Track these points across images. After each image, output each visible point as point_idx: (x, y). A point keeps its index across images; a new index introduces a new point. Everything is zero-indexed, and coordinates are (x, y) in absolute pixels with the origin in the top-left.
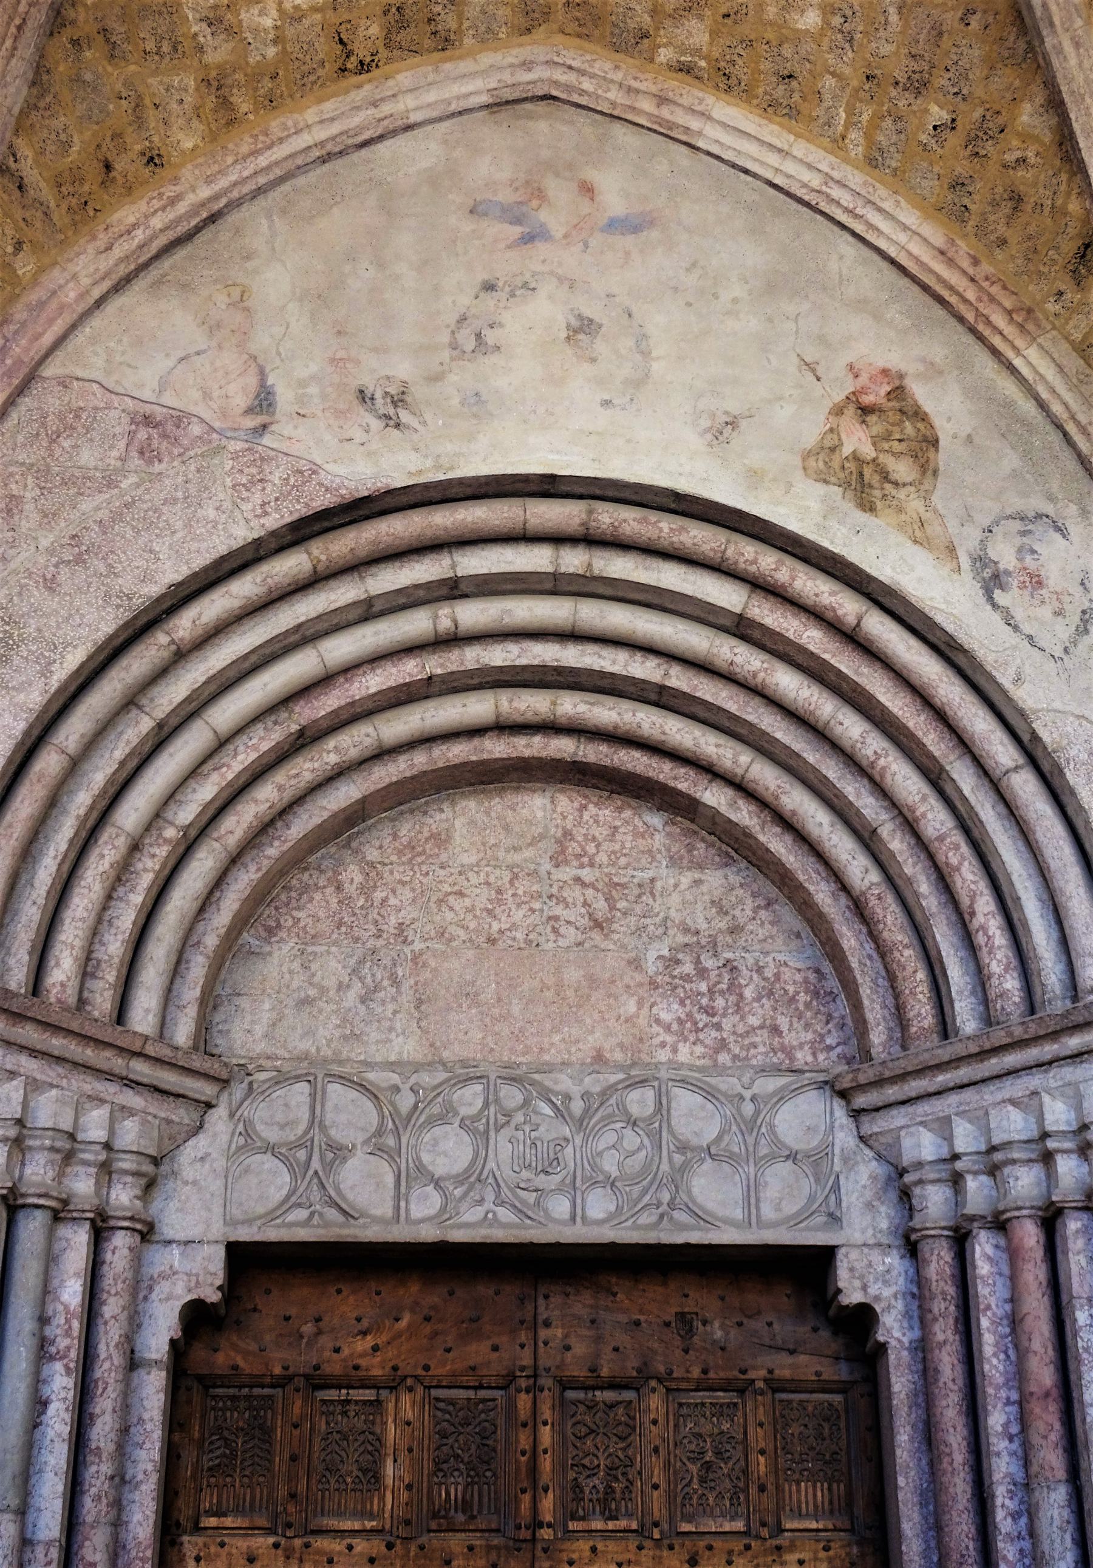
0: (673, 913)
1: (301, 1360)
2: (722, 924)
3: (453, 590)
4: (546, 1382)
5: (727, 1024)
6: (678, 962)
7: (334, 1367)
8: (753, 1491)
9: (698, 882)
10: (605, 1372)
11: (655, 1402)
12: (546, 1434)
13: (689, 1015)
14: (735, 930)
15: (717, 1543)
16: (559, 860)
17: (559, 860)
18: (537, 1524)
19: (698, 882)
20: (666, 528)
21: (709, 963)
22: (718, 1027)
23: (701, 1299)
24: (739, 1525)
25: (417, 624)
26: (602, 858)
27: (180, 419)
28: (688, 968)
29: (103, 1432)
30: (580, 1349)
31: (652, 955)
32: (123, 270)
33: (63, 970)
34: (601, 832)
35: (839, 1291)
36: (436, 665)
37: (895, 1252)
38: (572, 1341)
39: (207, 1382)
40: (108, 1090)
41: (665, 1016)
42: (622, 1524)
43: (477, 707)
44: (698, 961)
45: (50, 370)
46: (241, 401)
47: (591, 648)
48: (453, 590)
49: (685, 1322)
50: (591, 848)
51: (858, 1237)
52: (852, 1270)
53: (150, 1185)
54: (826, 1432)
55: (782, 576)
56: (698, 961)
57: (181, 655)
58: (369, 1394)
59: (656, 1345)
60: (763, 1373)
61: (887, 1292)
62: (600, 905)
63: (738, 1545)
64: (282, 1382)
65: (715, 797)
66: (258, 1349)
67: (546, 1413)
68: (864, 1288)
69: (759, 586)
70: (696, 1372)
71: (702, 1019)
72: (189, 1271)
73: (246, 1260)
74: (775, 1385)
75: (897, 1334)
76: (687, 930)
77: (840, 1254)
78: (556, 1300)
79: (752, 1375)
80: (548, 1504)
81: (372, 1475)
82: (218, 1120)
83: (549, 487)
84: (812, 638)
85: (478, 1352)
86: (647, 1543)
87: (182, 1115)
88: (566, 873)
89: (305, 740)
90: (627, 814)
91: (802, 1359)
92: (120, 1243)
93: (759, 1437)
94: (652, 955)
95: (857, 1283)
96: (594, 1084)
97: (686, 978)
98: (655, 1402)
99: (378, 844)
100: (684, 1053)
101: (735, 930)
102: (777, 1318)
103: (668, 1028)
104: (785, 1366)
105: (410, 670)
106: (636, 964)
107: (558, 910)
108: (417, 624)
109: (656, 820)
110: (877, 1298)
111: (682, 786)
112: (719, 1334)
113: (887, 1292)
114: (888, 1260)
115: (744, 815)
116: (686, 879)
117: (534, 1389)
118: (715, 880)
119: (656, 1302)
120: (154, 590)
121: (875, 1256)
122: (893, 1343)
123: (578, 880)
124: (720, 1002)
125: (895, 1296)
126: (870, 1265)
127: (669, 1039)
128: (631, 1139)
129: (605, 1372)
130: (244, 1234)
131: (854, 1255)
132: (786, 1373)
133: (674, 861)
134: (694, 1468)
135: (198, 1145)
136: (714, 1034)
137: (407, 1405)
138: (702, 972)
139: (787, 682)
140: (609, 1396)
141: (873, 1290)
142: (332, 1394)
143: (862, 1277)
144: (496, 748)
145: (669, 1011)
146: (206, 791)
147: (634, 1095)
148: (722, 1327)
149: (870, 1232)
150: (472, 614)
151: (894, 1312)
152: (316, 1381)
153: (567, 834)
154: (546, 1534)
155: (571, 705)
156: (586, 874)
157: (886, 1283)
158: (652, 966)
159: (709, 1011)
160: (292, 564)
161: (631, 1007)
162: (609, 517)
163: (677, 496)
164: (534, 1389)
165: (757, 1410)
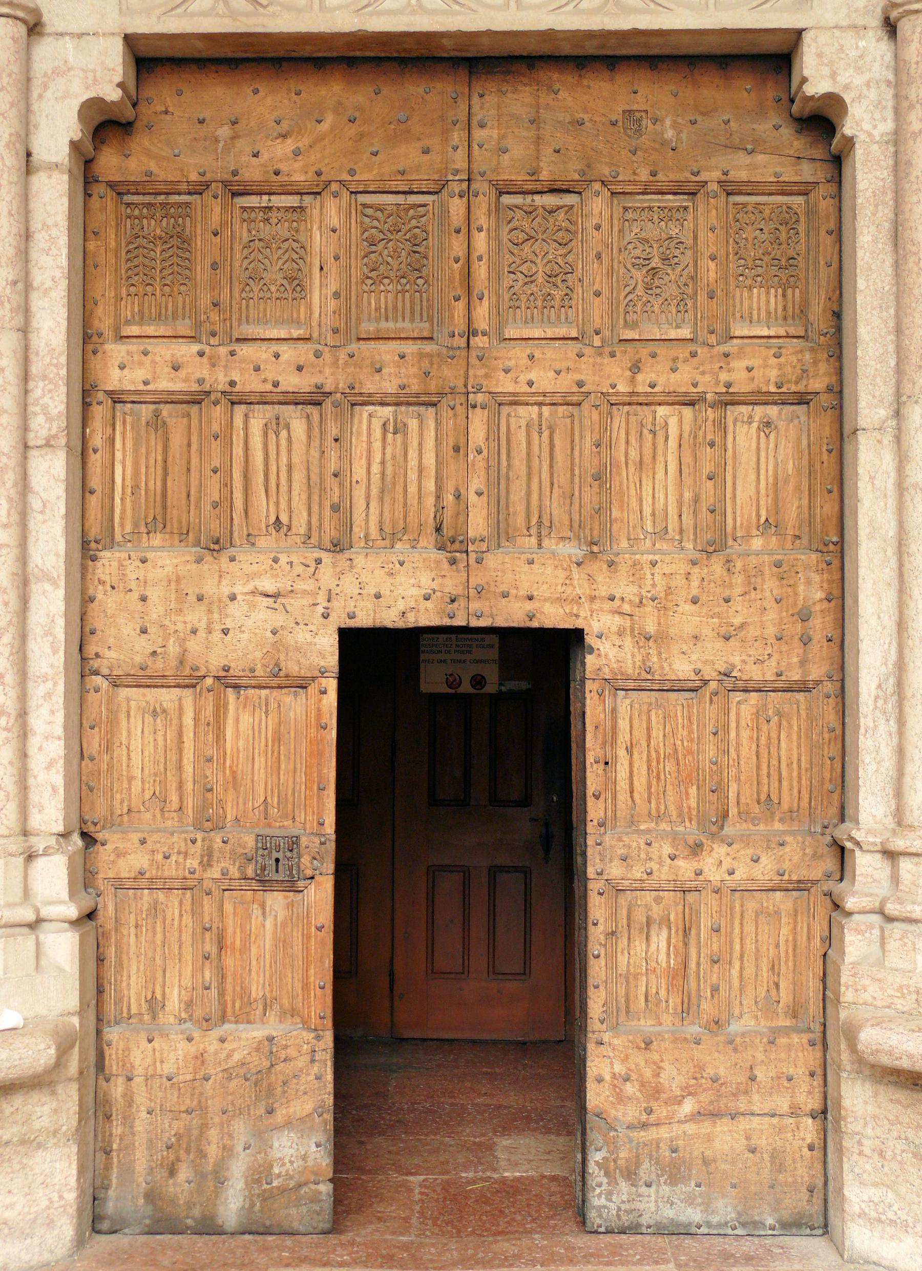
4: (480, 185)
7: (252, 172)
8: (702, 297)
10: (544, 175)
11: (598, 205)
12: (481, 242)
15: (661, 350)
18: (471, 332)
23: (652, 95)
24: (685, 332)
30: (519, 150)
35: (804, 80)
37: (871, 33)
38: (509, 142)
39: (119, 189)
42: (562, 332)
51: (830, 18)
52: (820, 55)
54: (783, 237)
58: (291, 201)
59: (601, 146)
60: (716, 175)
61: (859, 80)
63: (683, 352)
64: (200, 189)
67: (481, 218)
68: (833, 76)
70: (644, 175)
73: (150, 60)
74: (730, 189)
75: (866, 126)
77: (807, 38)
78: (491, 99)
79: (703, 177)
81: (296, 284)
85: (408, 155)
86: (587, 351)
91: (760, 158)
93: (709, 242)
95: (826, 71)
98: (598, 205)
102: (736, 101)
104: (742, 168)
110: (847, 87)
112: (670, 134)
113: (859, 80)
114: (862, 44)
117: (468, 194)
121: (848, 39)
122: (861, 137)
125: (868, 84)
126: (841, 49)
129: (544, 175)
130: (144, 25)
131: (824, 38)
132: (743, 175)
134: (638, 275)
137: (332, 210)
140: (550, 200)
141: (842, 79)
142: (252, 201)
143: (831, 63)
148: (675, 125)
149: (844, 11)
151: (865, 102)
152: (236, 189)
154: (479, 341)
157: (859, 70)
164: (468, 194)
165: (707, 215)
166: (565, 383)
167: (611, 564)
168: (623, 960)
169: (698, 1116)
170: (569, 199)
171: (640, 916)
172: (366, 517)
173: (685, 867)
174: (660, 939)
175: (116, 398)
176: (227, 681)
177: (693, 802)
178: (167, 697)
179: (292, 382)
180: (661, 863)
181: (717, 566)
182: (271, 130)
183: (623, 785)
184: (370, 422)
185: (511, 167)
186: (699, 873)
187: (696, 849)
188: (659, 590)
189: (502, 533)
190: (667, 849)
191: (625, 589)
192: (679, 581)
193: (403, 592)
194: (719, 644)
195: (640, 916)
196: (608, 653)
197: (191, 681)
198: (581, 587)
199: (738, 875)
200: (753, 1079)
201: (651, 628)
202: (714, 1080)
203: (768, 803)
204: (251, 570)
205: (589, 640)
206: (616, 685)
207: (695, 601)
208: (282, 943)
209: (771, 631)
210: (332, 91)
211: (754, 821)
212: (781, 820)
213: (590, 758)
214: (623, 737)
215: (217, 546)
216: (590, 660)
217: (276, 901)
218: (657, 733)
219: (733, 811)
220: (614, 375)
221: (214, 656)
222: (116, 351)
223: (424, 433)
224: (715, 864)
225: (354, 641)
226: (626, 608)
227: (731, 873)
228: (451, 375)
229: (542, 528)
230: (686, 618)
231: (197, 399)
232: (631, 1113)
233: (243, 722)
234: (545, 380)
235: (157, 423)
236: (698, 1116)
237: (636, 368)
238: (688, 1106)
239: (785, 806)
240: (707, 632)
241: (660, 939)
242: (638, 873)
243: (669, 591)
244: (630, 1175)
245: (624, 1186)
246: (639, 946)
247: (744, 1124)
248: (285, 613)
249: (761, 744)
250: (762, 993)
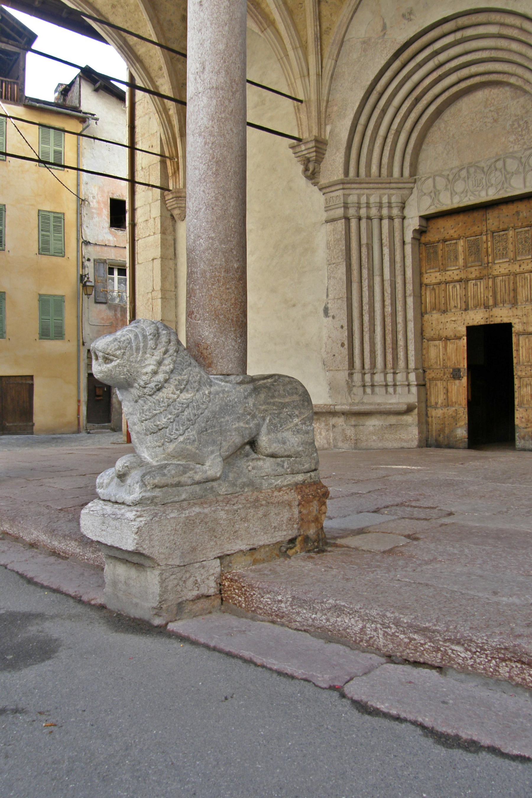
0: (513, 113)
1: (441, 237)
2: (524, 111)
3: (436, 53)
4: (489, 232)
5: (526, 138)
6: (514, 125)
7: (447, 237)
9: (518, 102)
10: (501, 228)
12: (489, 244)
13: (517, 138)
14: (527, 112)
16: (485, 107)
17: (485, 107)
18: (488, 263)
19: (518, 102)
20: (474, 19)
21: (521, 123)
22: (523, 139)
25: (430, 65)
26: (496, 103)
27: (370, 39)
28: (516, 126)
29: (398, 258)
30: (496, 224)
31: (508, 125)
32: (354, 8)
33: (374, 169)
34: (494, 96)
36: (440, 72)
39: (425, 244)
40: (387, 191)
41: (511, 140)
42: (506, 260)
43: (453, 78)
44: (518, 123)
45: (345, 39)
46: (380, 29)
47: (473, 54)
48: (436, 53)
49: (518, 213)
50: (493, 101)
53: (403, 208)
55: (502, 21)
56: (518, 123)
57: (381, 94)
58: (455, 241)
62: (496, 116)
64: (438, 242)
65: (512, 80)
66: (432, 236)
67: (489, 239)
69: (502, 24)
70: (520, 224)
71: (520, 138)
72: (413, 223)
73: (427, 219)
76: (515, 116)
78: (490, 214)
80: (490, 258)
81: (456, 258)
82: (415, 191)
83: (445, 20)
84: (515, 33)
85: (475, 229)
87: (406, 192)
88: (487, 110)
89: (417, 100)
90: (501, 89)
92: (397, 222)
94: (508, 125)
96: (489, 163)
97: (516, 128)
98: (511, 233)
99: (447, 115)
100: (516, 148)
101: (527, 112)
103: (512, 143)
105: (435, 75)
106: (504, 128)
107: (486, 120)
108: (430, 65)
109: (507, 89)
111: (505, 80)
112: (525, 214)
115: (520, 83)
116: (515, 102)
117: (487, 235)
118: (522, 100)
119: (512, 208)
120: (369, 83)
123: (490, 111)
124: (524, 132)
127: (512, 145)
128: (498, 173)
129: (501, 228)
133: (513, 99)
135: (412, 197)
136: (523, 141)
137: (461, 243)
138: (519, 126)
139: (515, 46)
142: (448, 243)
144: (463, 85)
145: (512, 138)
146: (397, 120)
147: (498, 163)
150: (442, 57)
152: (445, 241)
153: (487, 99)
154: (490, 264)
155: (474, 69)
156: (492, 109)
158: (508, 127)
159: (521, 135)
160: (397, 64)
161: (504, 139)
162: (461, 21)
163: (475, 10)
164: (487, 235)
166: (507, 271)
170: (506, 232)
171: (525, 383)
172: (471, 303)
175: (426, 285)
176: (447, 339)
178: (437, 342)
179: (456, 278)
182: (448, 228)
183: (521, 355)
184: (471, 284)
185: (494, 228)
189: (495, 305)
191: (519, 313)
193: (478, 318)
196: (517, 328)
197: (440, 339)
198: (511, 314)
204: (450, 317)
205: (513, 325)
206: (519, 334)
208: (458, 390)
210: (461, 218)
214: (521, 345)
215: (445, 312)
216: (513, 329)
217: (457, 382)
218: (527, 344)
220: (516, 268)
221: (444, 334)
222: (425, 276)
223: (482, 285)
225: (470, 329)
228: (485, 272)
229: (504, 302)
231: (439, 284)
232: (523, 425)
233: (451, 346)
234: (503, 271)
235: (434, 289)
237: (520, 266)
242: (524, 374)
243: (528, 313)
244: (523, 438)
245: (522, 441)
248: (456, 324)
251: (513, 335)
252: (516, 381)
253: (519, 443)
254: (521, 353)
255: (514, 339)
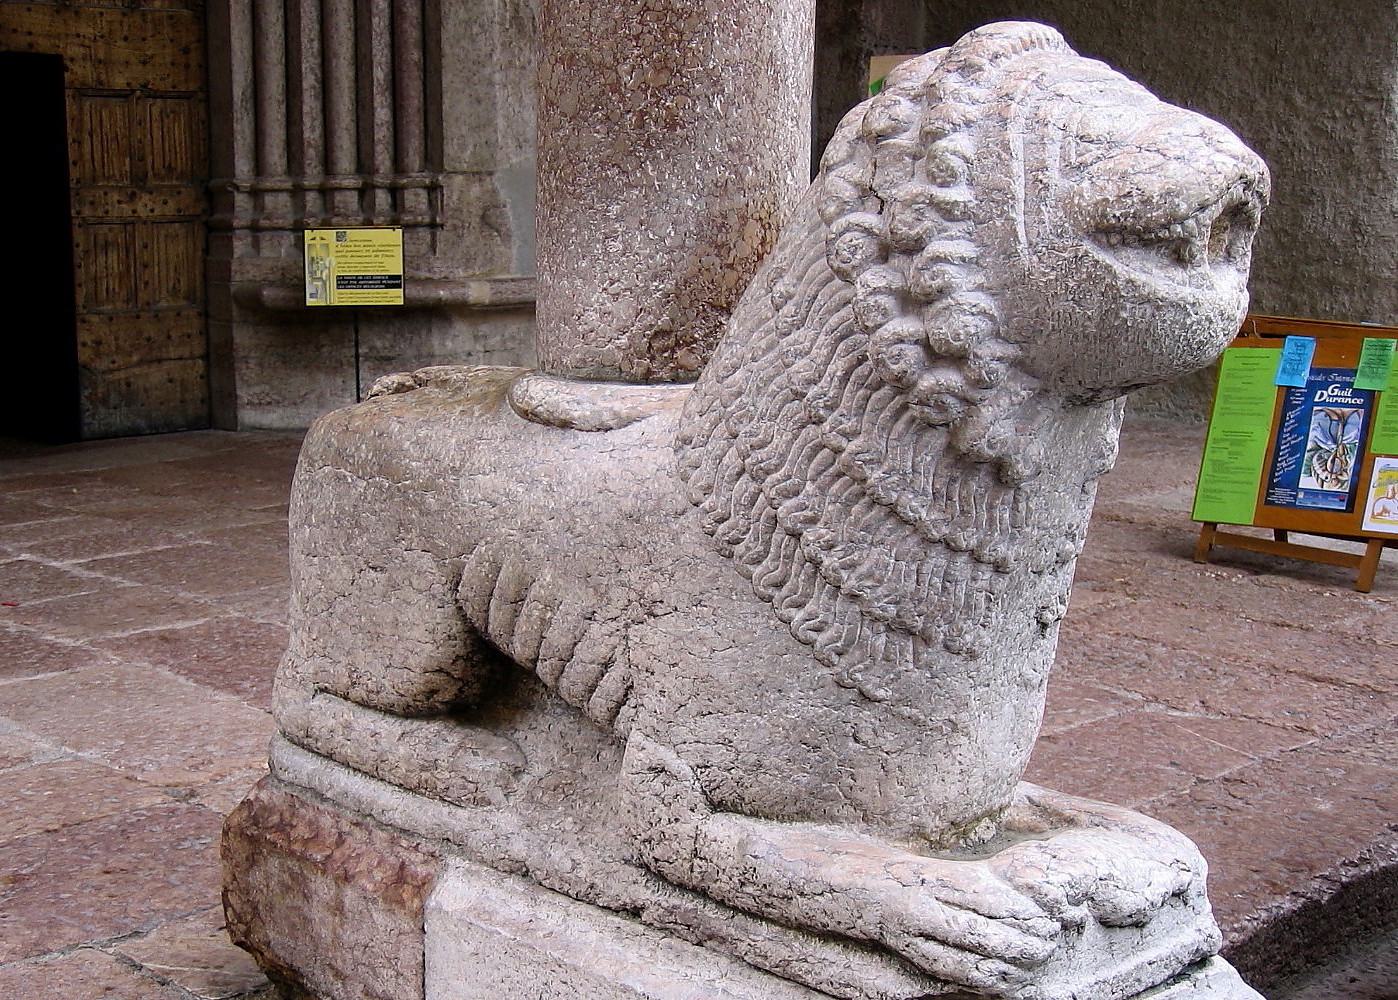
167: (77, 13)
168: (93, 269)
169: (140, 363)
173: (126, 209)
174: (113, 257)
177: (128, 168)
180: (113, 206)
181: (137, 18)
186: (134, 212)
187: (132, 197)
188: (105, 31)
190: (116, 197)
191: (87, 31)
192: (116, 26)
194: (140, 67)
195: (101, 241)
196: (80, 71)
199: (156, 212)
200: (169, 337)
201: (101, 55)
202: (149, 339)
203: (170, 169)
206: (82, 92)
207: (126, 39)
209: (168, 59)
211: (163, 179)
212: (177, 179)
213: (70, 141)
218: (106, 124)
219: (150, 174)
224: (145, 206)
226: (87, 42)
227: (152, 211)
230: (121, 51)
236: (140, 363)
238: (135, 358)
239: (179, 170)
240: (133, 59)
241: (113, 257)
242: (100, 213)
244: (105, 402)
245: (102, 410)
246: (101, 259)
247: (166, 366)
249: (167, 134)
250: (171, 285)
251: (68, 92)
252: (79, 236)
253: (95, 418)
254: (87, 148)
255: (71, 108)
